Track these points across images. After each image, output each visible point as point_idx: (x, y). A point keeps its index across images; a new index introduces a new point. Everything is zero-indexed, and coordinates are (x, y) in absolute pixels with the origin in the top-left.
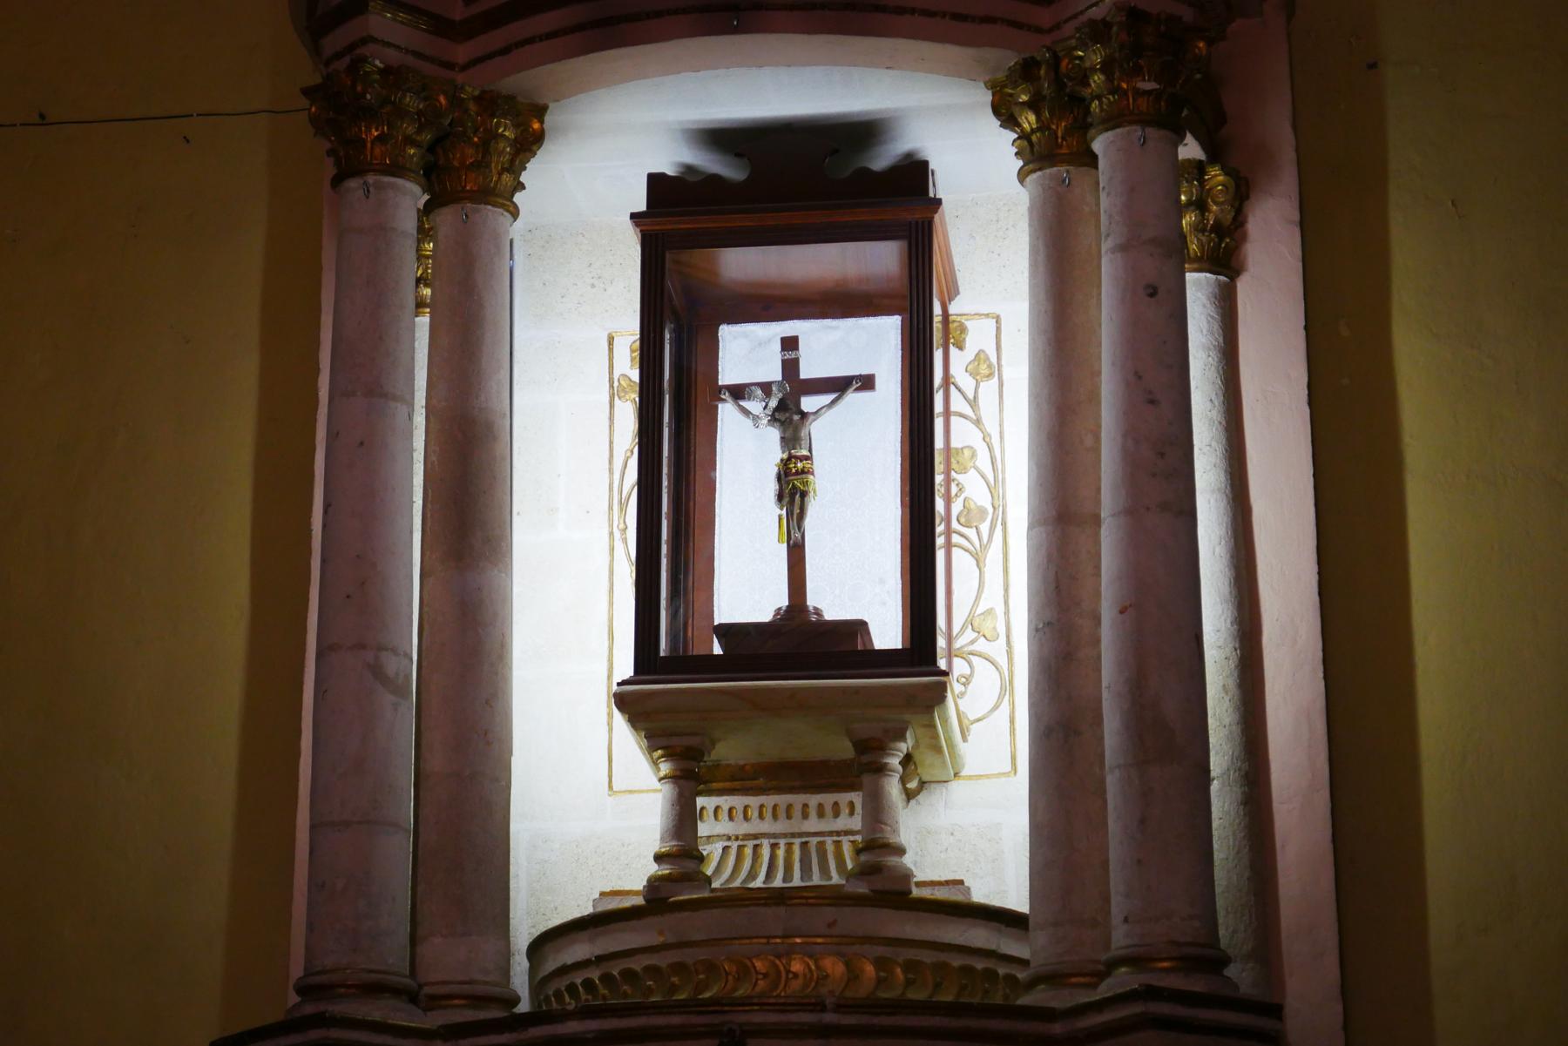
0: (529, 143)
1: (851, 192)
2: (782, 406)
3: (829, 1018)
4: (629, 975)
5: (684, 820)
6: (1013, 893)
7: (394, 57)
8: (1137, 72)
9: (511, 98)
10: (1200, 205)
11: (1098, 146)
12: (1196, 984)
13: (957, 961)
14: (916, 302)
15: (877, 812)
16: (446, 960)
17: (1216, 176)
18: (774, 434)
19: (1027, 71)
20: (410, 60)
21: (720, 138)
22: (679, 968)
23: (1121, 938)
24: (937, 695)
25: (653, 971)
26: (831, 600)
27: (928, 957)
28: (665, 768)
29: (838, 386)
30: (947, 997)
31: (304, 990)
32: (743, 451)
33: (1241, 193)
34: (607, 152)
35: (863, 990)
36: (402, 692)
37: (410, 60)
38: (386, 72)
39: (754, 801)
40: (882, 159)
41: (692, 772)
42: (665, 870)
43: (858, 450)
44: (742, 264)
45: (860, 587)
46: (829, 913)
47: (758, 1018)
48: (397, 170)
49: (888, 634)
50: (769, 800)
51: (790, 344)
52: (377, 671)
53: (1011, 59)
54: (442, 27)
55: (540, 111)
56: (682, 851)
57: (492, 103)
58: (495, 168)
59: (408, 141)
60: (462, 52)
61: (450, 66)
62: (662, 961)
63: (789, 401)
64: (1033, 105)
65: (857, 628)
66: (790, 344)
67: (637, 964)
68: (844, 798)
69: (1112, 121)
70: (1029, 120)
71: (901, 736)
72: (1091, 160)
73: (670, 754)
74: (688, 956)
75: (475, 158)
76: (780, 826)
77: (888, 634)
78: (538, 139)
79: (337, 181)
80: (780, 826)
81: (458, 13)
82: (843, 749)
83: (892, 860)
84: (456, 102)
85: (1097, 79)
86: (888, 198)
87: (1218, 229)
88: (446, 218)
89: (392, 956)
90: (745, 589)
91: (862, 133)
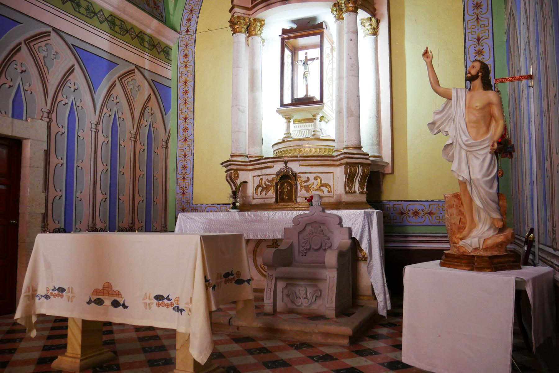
0: (262, 26)
1: (309, 27)
2: (304, 64)
3: (299, 158)
4: (281, 151)
5: (288, 128)
6: (333, 137)
7: (239, 15)
8: (349, 3)
9: (258, 19)
10: (371, 25)
11: (344, 15)
12: (355, 151)
13: (328, 148)
14: (321, 46)
15: (315, 126)
16: (254, 151)
17: (373, 19)
18: (303, 67)
19: (335, 5)
20: (242, 15)
21: (294, 22)
22: (287, 150)
23: (345, 145)
24: (323, 107)
25: (284, 151)
26: (311, 94)
27: (323, 147)
28: (286, 121)
29: (313, 59)
30: (326, 154)
31: (232, 156)
33: (378, 22)
35: (311, 154)
36: (243, 112)
37: (242, 15)
38: (238, 17)
39: (302, 124)
40: (319, 21)
42: (285, 136)
44: (302, 41)
46: (308, 142)
47: (288, 159)
48: (240, 32)
50: (304, 124)
51: (306, 53)
52: (239, 109)
53: (332, 4)
54: (247, 9)
55: (264, 20)
56: (288, 133)
57: (255, 20)
58: (257, 29)
59: (242, 27)
60: (251, 12)
61: (249, 15)
62: (285, 149)
63: (305, 63)
64: (336, 11)
65: (312, 98)
66: (306, 53)
67: (282, 150)
68: (310, 124)
69: (347, 11)
70: (335, 13)
71: (318, 114)
72: (343, 19)
73: (286, 118)
74: (288, 149)
76: (306, 128)
77: (319, 99)
78: (264, 24)
79: (233, 34)
80: (306, 128)
81: (250, 6)
82: (312, 117)
83: (317, 133)
84: (250, 20)
85: (343, 5)
87: (374, 29)
88: (250, 38)
91: (314, 19)
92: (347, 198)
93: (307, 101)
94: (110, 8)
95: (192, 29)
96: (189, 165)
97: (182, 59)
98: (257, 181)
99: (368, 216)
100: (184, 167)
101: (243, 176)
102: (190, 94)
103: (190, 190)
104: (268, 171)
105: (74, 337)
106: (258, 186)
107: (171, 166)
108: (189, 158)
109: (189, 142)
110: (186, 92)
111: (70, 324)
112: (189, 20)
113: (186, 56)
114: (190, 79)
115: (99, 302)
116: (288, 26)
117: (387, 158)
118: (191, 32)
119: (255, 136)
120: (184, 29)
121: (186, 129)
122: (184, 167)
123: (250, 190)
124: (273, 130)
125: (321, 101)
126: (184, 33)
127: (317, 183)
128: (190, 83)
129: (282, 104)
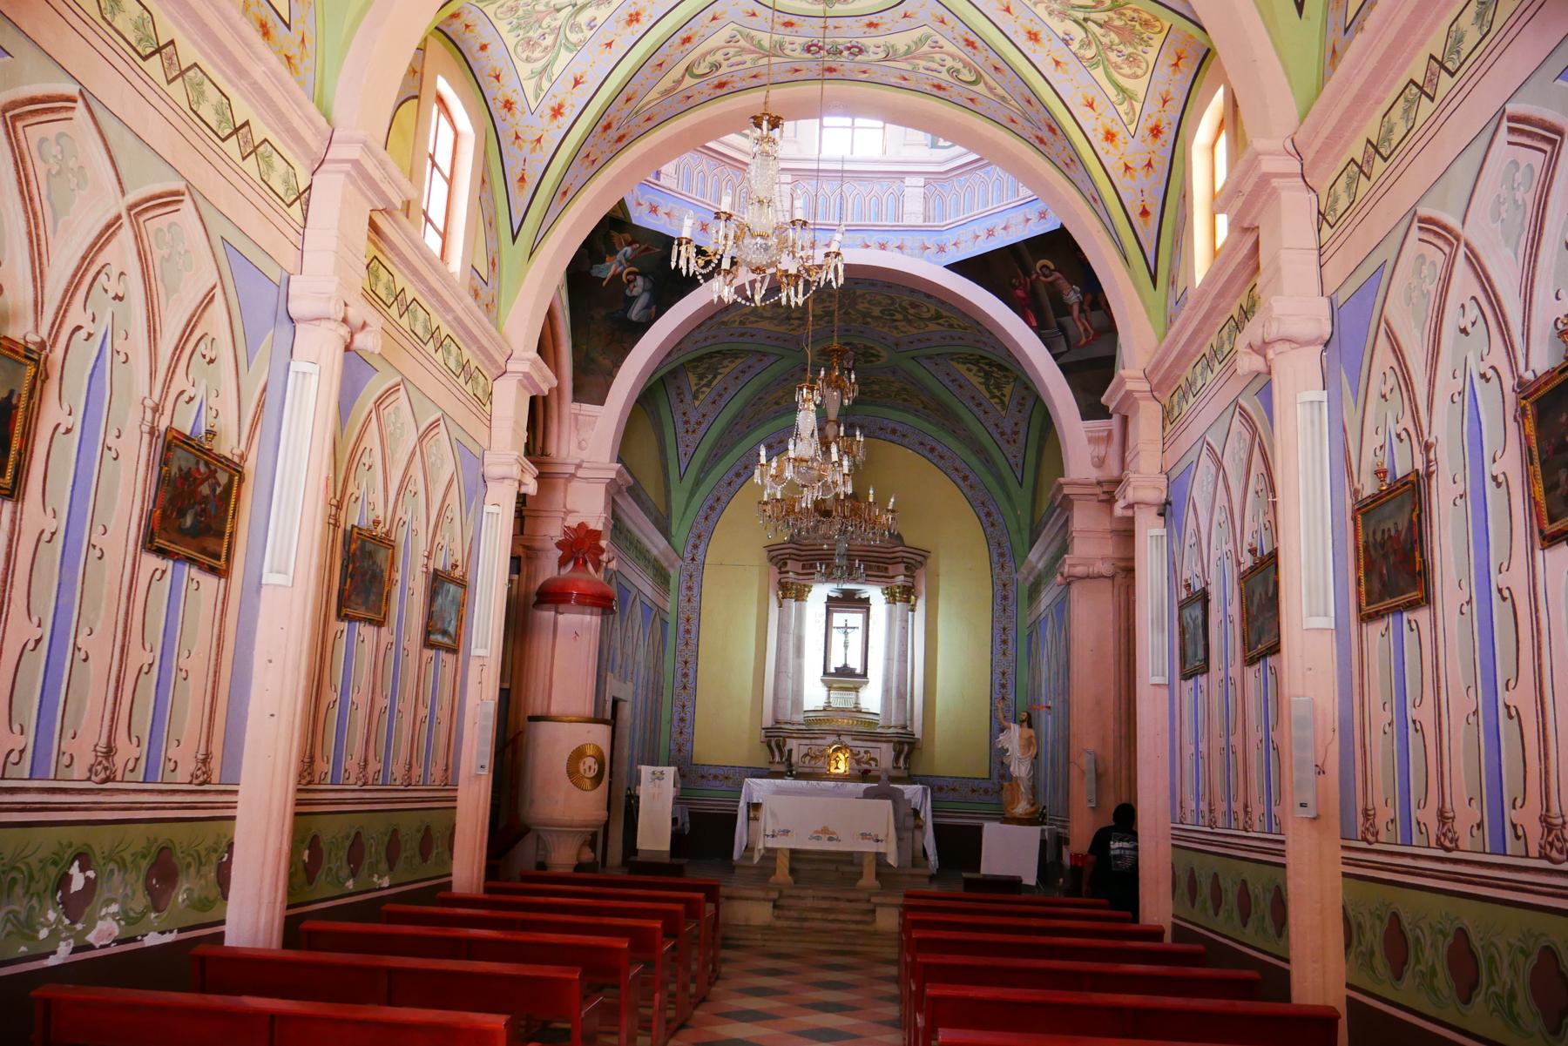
26: (851, 665)
32: (837, 637)
34: (820, 593)
41: (830, 688)
43: (856, 638)
45: (855, 664)
49: (858, 671)
63: (846, 629)
75: (800, 596)
86: (863, 604)
89: (788, 718)
90: (836, 662)
92: (894, 773)
93: (845, 671)
94: (655, 552)
95: (699, 557)
96: (688, 719)
97: (684, 591)
98: (804, 750)
99: (925, 790)
100: (682, 720)
101: (792, 744)
102: (693, 635)
103: (688, 748)
104: (819, 742)
105: (783, 864)
106: (806, 755)
107: (665, 716)
108: (689, 710)
109: (690, 691)
110: (688, 631)
111: (779, 854)
112: (695, 547)
113: (690, 588)
114: (694, 616)
115: (818, 838)
116: (834, 595)
117: (917, 729)
118: (698, 562)
119: (798, 700)
120: (688, 555)
121: (685, 675)
122: (682, 720)
123: (794, 759)
124: (815, 695)
125: (865, 675)
126: (688, 561)
127: (866, 757)
128: (694, 621)
129: (825, 673)
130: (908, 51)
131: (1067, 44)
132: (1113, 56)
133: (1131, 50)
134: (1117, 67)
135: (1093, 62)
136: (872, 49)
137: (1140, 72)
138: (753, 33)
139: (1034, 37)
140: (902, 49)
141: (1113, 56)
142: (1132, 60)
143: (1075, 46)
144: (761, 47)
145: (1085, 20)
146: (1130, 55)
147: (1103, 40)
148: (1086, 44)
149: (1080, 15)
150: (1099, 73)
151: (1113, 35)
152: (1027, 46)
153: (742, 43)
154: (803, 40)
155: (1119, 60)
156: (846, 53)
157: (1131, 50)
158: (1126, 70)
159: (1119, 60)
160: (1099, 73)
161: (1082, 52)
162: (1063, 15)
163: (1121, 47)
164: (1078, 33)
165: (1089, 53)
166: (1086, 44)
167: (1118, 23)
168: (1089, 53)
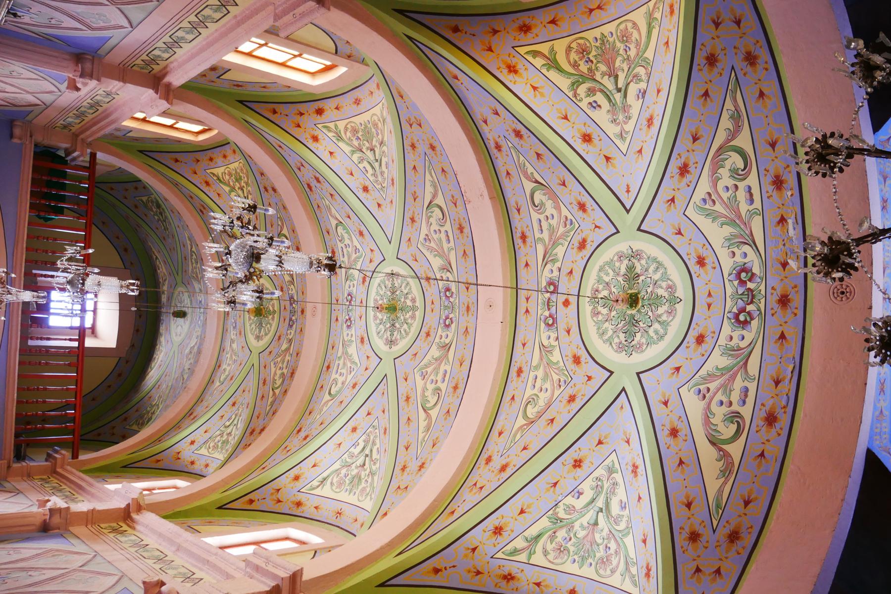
130: (732, 222)
131: (645, 92)
132: (632, 53)
133: (618, 44)
134: (638, 44)
135: (646, 64)
136: (739, 259)
137: (630, 25)
138: (703, 372)
139: (650, 121)
140: (728, 230)
141: (632, 53)
142: (625, 38)
143: (643, 85)
144: (727, 369)
145: (619, 90)
146: (623, 41)
147: (626, 69)
148: (637, 78)
149: (618, 97)
150: (649, 54)
151: (617, 64)
152: (656, 123)
153: (713, 386)
154: (727, 329)
155: (632, 46)
156: (750, 285)
157: (618, 44)
158: (635, 35)
159: (632, 46)
160: (649, 54)
161: (644, 77)
162: (626, 108)
163: (622, 52)
164: (633, 89)
165: (641, 71)
166: (637, 78)
167: (603, 68)
168: (641, 71)
